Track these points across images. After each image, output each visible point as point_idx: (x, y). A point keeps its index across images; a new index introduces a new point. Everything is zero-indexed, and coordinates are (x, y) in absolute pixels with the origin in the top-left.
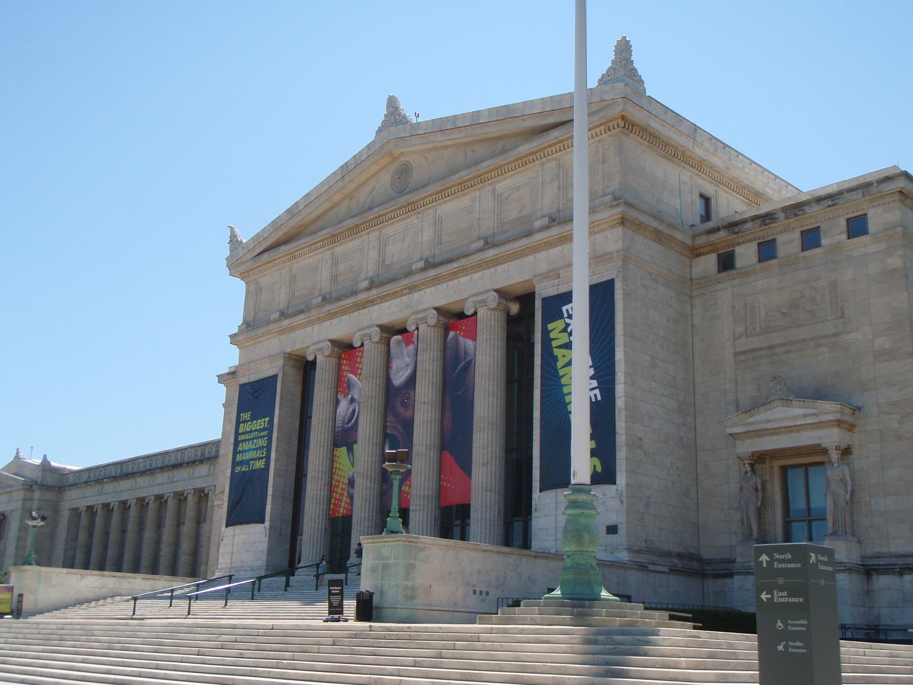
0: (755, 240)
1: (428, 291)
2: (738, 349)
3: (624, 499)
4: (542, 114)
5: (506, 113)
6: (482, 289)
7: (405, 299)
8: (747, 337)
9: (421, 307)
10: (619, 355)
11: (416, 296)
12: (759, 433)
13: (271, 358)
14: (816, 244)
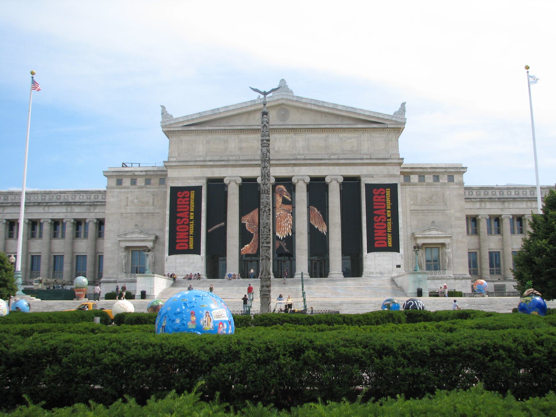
0: (417, 174)
1: (304, 168)
2: (411, 209)
3: (403, 257)
4: (369, 116)
5: (352, 110)
6: (335, 174)
7: (290, 168)
8: (415, 205)
9: (300, 174)
10: (400, 210)
11: (296, 169)
12: (426, 238)
13: (196, 178)
14: (438, 181)
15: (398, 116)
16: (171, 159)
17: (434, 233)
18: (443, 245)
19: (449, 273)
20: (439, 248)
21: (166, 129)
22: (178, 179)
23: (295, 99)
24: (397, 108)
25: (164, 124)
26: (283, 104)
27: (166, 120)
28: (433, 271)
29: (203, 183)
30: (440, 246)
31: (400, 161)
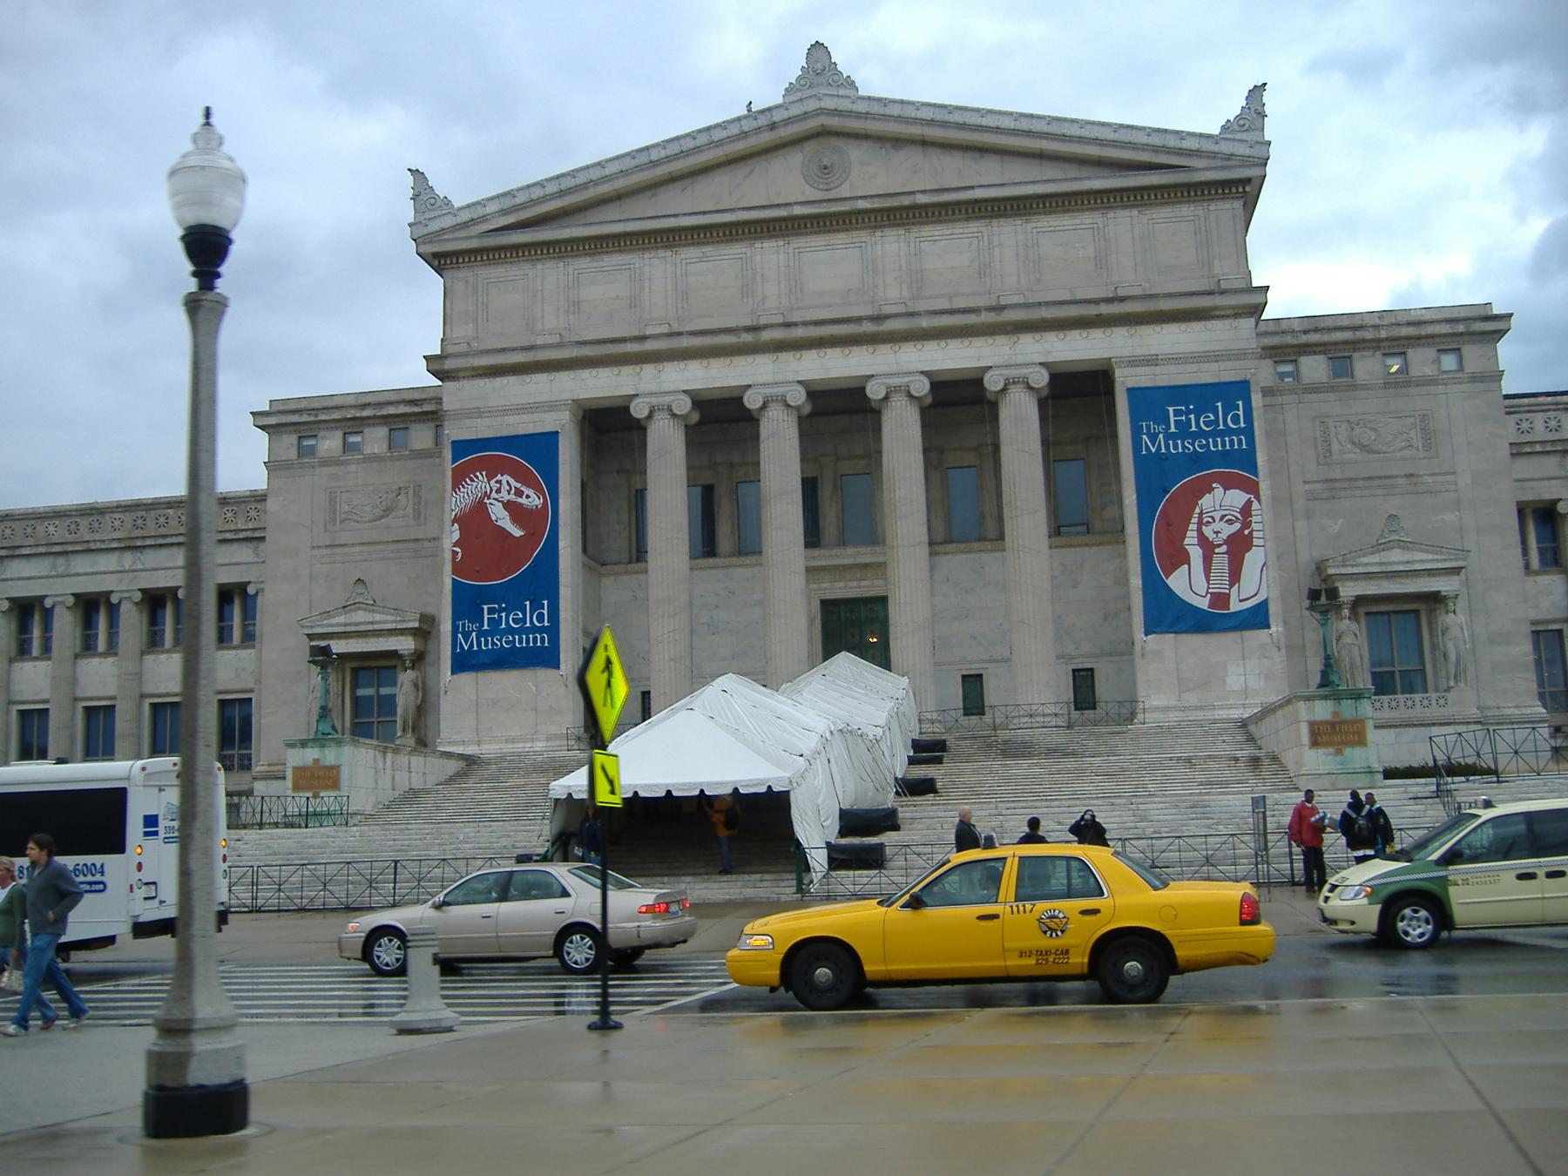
15: (1238, 136)
16: (450, 349)
17: (1396, 558)
18: (1435, 600)
19: (1463, 702)
20: (1416, 612)
21: (429, 249)
22: (477, 413)
23: (861, 107)
24: (1233, 107)
25: (422, 231)
26: (824, 133)
27: (427, 215)
28: (1401, 697)
29: (561, 422)
30: (1422, 607)
31: (1254, 299)
